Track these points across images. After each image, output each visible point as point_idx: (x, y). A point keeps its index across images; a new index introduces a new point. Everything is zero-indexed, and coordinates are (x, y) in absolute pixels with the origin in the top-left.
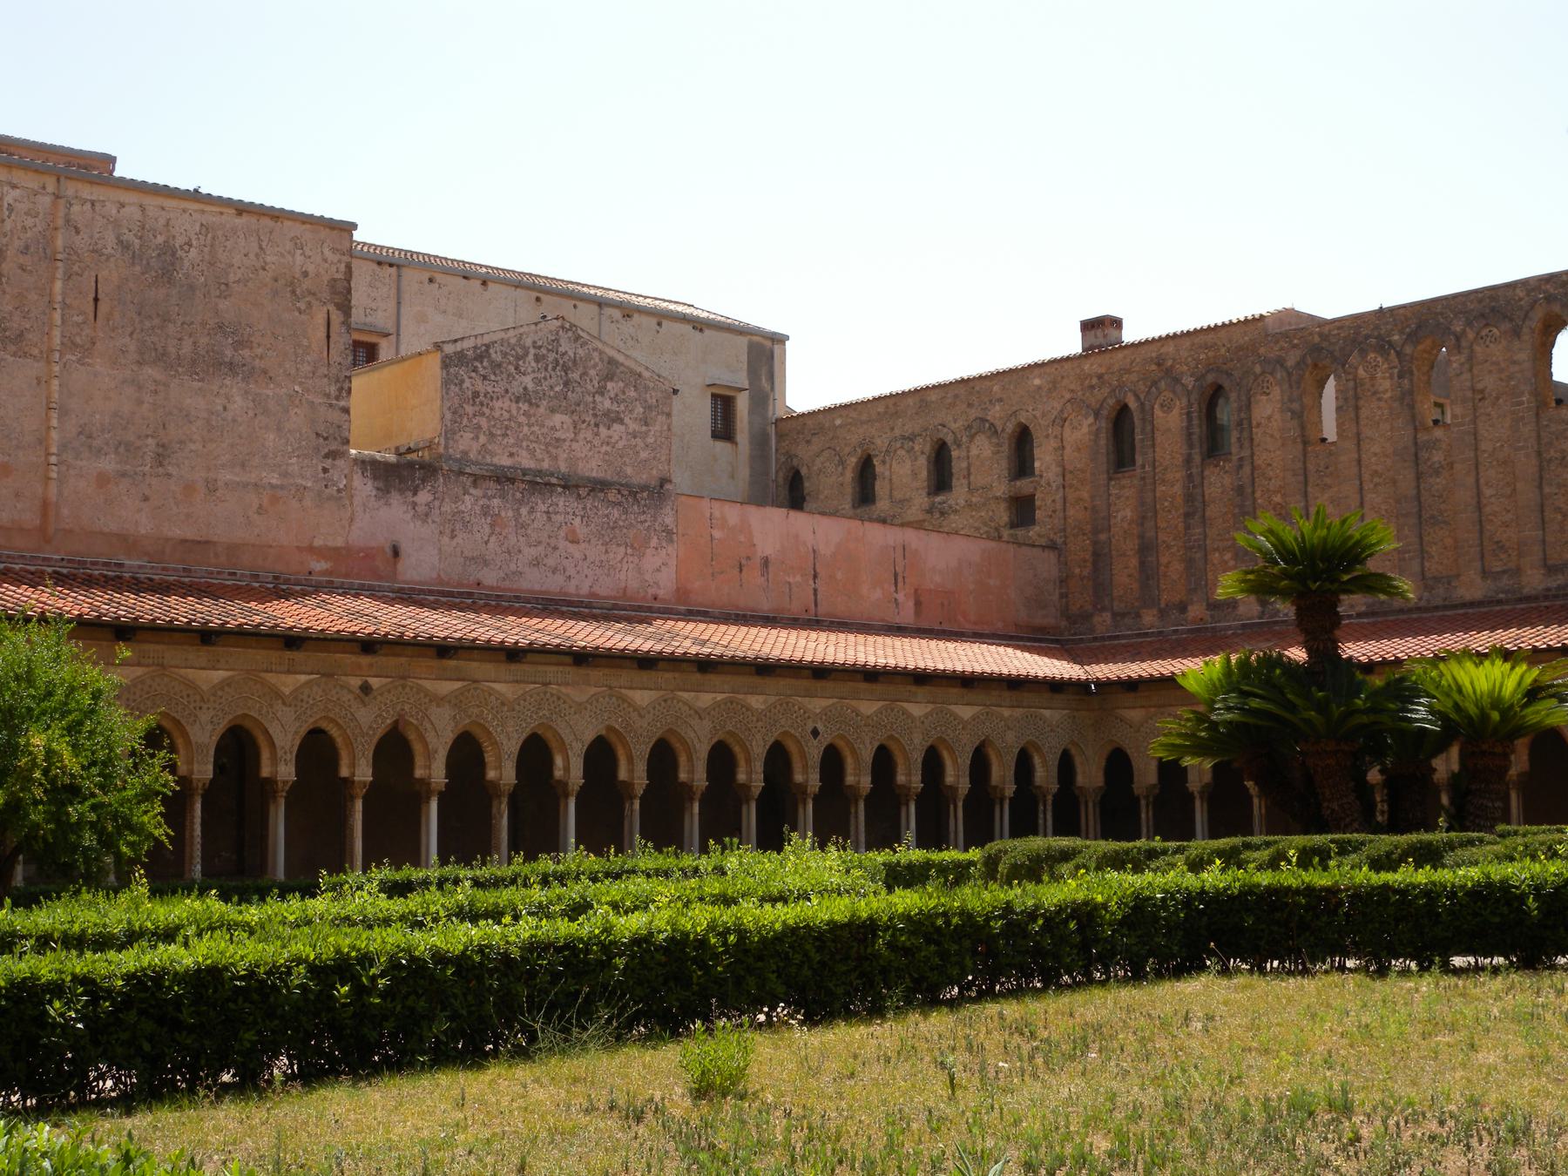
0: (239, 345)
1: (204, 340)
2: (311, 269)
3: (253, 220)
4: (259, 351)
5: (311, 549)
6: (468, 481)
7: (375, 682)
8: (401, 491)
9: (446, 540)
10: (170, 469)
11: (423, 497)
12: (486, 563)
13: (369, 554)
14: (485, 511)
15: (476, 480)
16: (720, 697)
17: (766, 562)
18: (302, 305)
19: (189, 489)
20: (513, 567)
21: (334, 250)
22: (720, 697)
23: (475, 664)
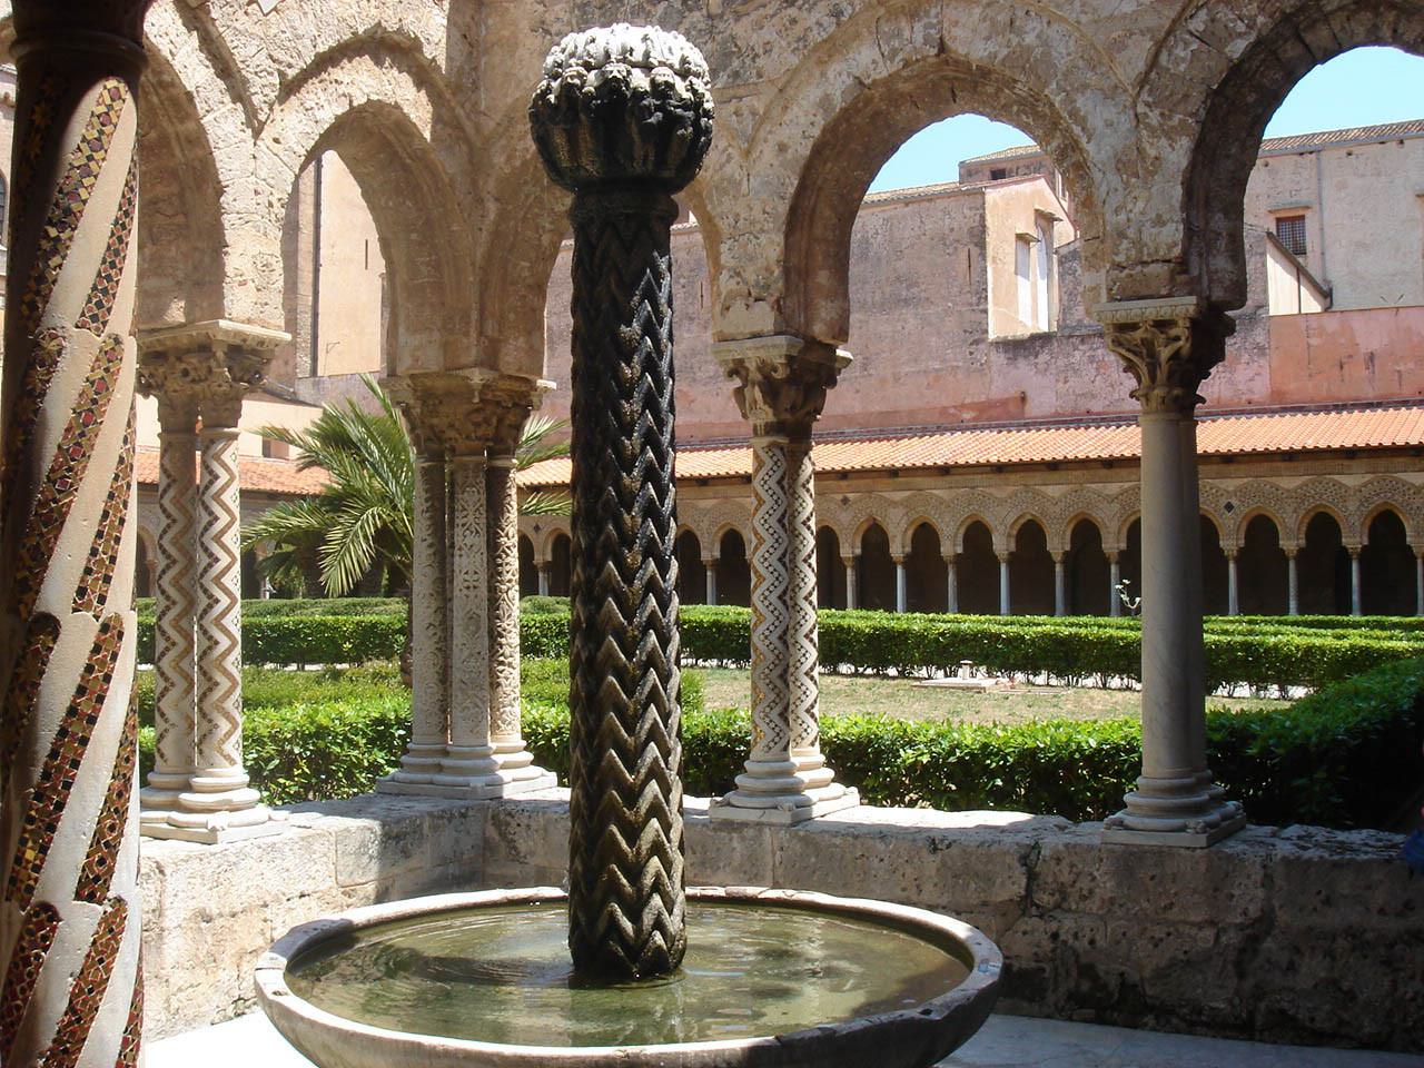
0: (909, 287)
1: (888, 290)
2: (956, 225)
3: (916, 205)
4: (923, 287)
5: (963, 407)
6: (1076, 341)
7: (851, 496)
8: (1026, 357)
9: (1061, 384)
10: (872, 371)
11: (1043, 357)
12: (1094, 396)
13: (1004, 403)
14: (1092, 360)
15: (1083, 339)
16: (1127, 485)
17: (1372, 357)
18: (951, 250)
19: (883, 381)
20: (1116, 396)
21: (971, 209)
22: (1127, 485)
23: (919, 479)
